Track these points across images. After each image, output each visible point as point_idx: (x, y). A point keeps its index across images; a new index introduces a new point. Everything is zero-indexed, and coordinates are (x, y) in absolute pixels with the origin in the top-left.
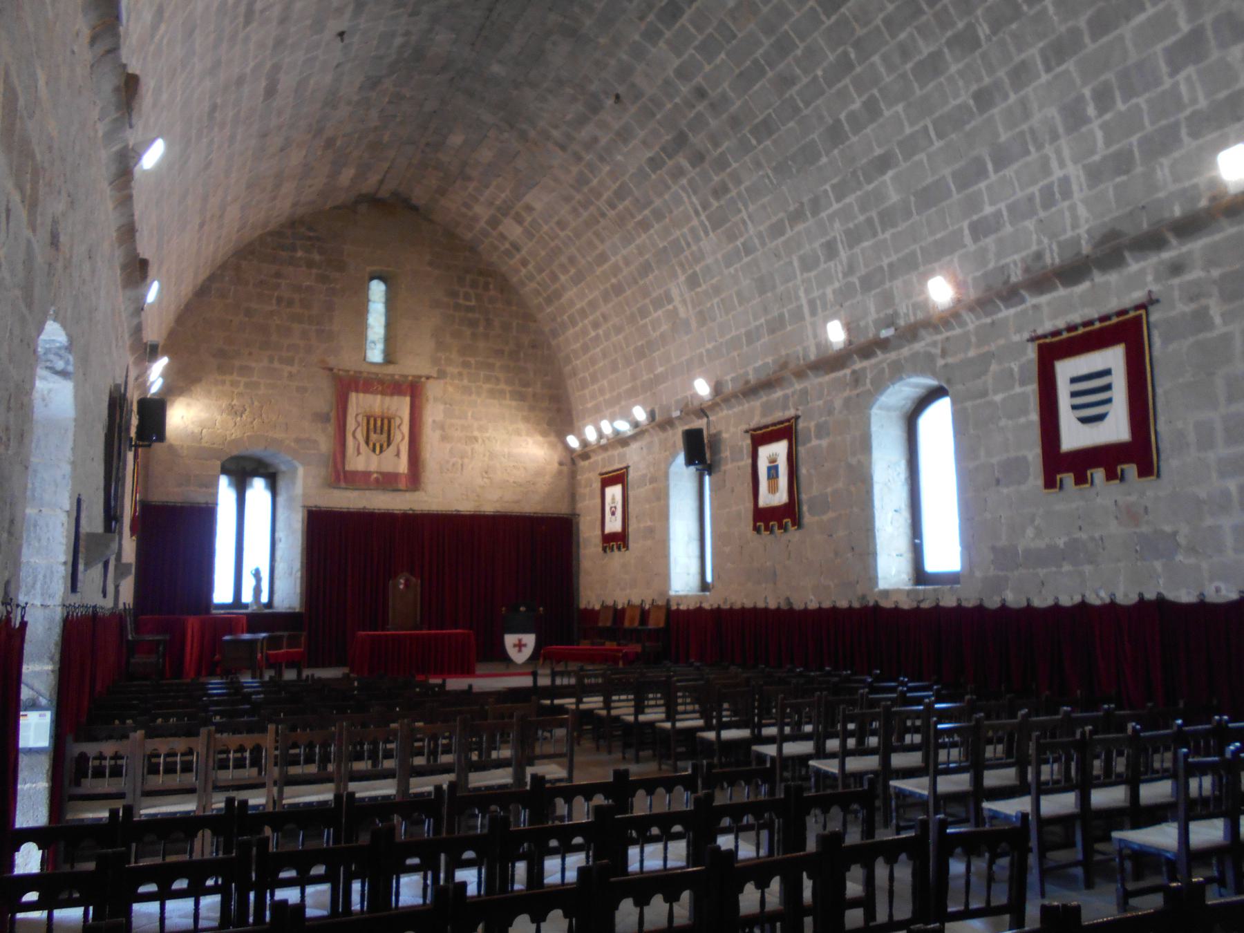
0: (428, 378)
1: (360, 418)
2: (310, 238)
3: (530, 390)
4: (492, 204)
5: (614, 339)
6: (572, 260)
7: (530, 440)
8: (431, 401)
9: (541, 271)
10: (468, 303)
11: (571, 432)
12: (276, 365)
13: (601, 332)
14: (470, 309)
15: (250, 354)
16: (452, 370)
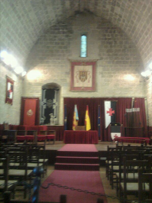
0: (98, 60)
2: (63, 26)
3: (129, 60)
4: (110, 2)
6: (136, 13)
9: (128, 22)
14: (110, 39)
16: (104, 57)
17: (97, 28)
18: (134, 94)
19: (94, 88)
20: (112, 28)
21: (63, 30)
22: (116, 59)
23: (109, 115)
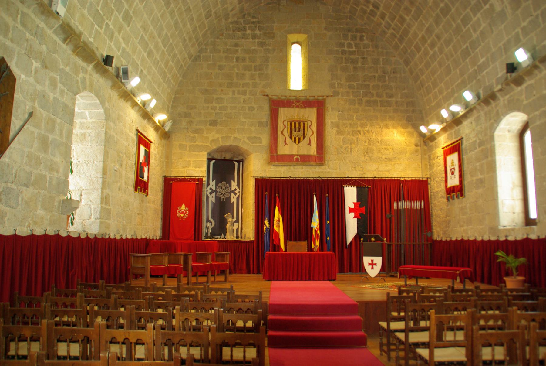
0: (328, 96)
1: (285, 123)
2: (254, 22)
3: (393, 99)
5: (446, 50)
7: (395, 131)
8: (330, 110)
9: (393, 19)
10: (351, 50)
11: (424, 125)
12: (236, 95)
13: (436, 49)
15: (222, 90)
17: (326, 29)
18: (404, 170)
19: (320, 157)
20: (357, 31)
21: (253, 30)
22: (365, 95)
23: (354, 216)
